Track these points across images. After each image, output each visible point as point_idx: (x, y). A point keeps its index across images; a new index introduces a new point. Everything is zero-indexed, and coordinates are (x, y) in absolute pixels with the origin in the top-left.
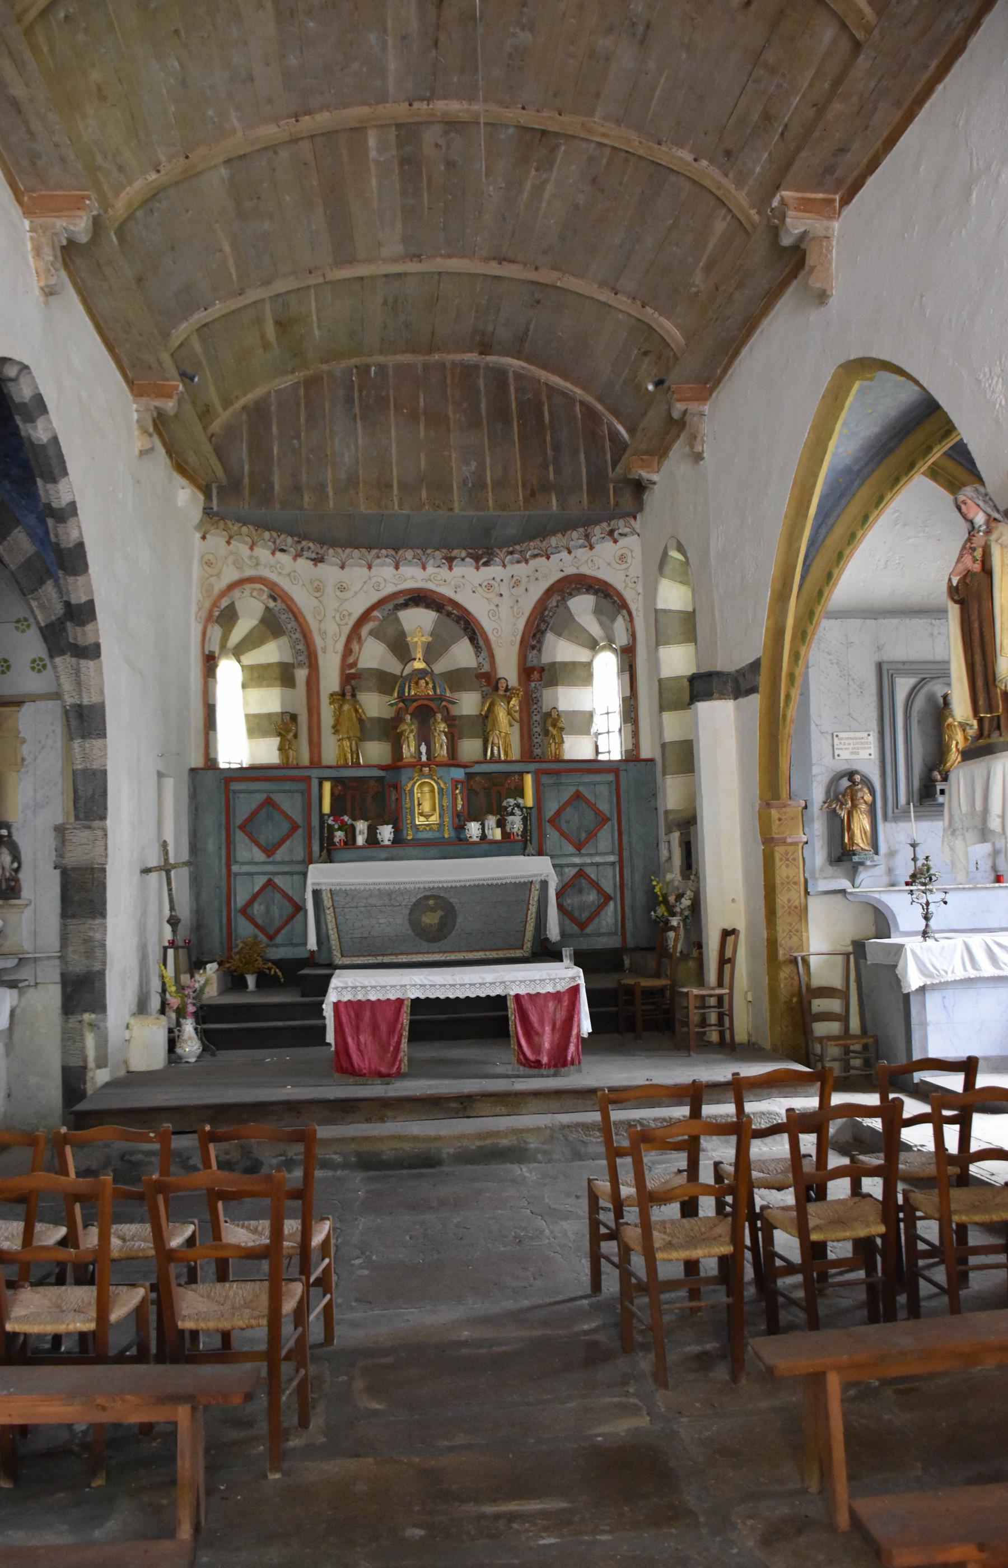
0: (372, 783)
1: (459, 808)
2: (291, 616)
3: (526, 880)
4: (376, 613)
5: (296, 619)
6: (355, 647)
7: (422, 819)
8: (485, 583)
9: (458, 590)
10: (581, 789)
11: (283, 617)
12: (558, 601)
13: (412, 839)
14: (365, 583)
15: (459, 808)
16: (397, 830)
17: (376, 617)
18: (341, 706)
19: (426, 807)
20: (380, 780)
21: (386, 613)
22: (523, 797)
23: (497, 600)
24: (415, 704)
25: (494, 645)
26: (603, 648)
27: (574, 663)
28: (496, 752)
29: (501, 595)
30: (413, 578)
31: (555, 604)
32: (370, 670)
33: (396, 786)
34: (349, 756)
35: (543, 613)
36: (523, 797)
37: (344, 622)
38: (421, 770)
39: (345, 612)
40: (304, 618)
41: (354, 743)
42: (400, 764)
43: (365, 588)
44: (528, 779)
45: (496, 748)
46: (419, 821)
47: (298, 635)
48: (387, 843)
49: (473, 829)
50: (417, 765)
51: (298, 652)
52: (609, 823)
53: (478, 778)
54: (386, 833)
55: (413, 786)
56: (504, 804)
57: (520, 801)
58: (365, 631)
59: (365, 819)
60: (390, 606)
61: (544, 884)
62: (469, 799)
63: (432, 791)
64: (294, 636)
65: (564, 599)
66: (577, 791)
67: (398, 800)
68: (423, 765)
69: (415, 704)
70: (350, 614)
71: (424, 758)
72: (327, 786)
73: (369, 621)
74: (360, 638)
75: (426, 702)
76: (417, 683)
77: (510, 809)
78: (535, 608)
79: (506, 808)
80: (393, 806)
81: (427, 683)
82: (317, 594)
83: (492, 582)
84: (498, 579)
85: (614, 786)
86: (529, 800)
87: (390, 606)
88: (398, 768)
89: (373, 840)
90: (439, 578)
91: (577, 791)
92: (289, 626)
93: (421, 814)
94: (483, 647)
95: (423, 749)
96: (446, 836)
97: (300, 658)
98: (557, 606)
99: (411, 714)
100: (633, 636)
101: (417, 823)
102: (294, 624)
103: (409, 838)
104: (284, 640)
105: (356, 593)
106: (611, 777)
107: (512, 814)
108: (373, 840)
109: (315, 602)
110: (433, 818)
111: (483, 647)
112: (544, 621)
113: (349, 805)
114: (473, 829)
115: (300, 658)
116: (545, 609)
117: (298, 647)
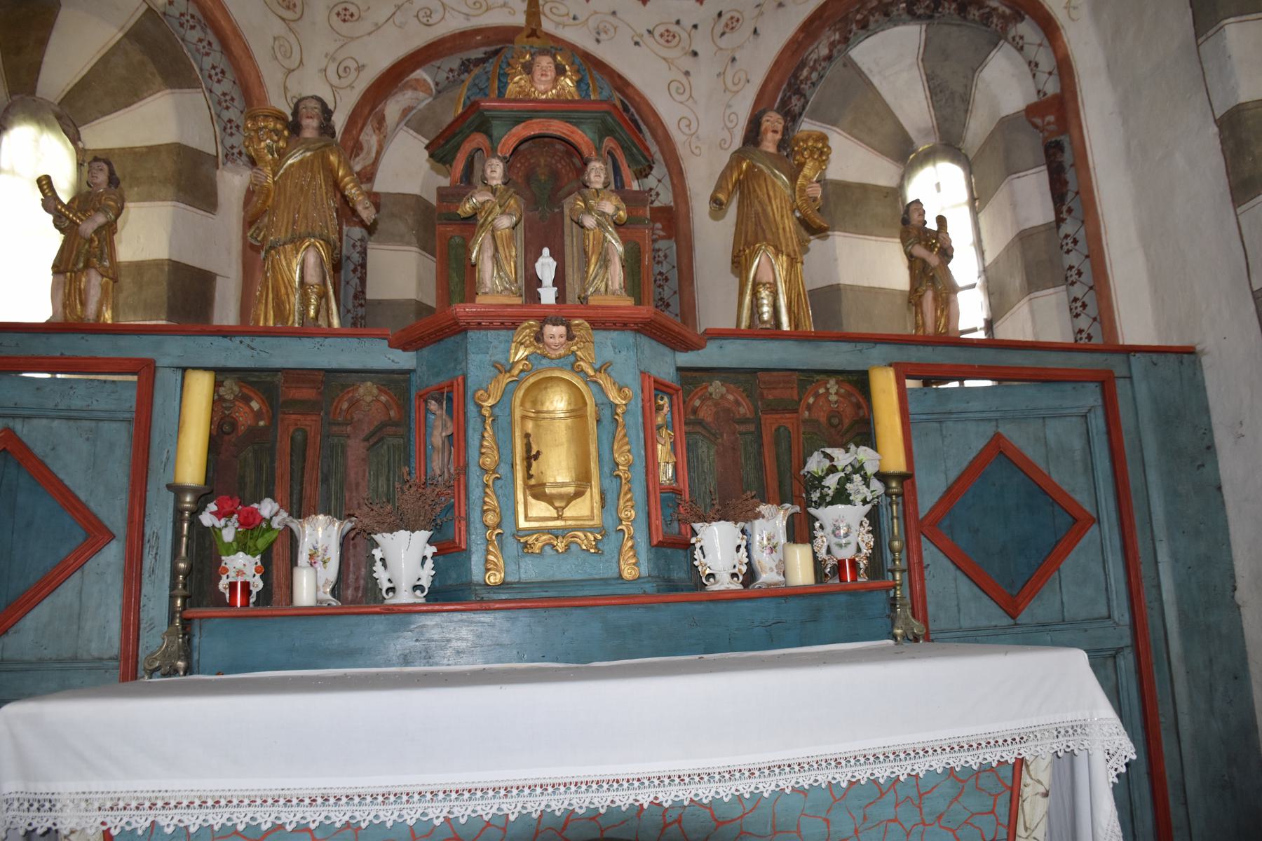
0: (366, 391)
1: (666, 474)
2: (211, 37)
3: (993, 756)
4: (420, 74)
5: (226, 48)
6: (370, 139)
7: (540, 509)
8: (661, 29)
9: (603, 36)
10: (1007, 430)
11: (193, 36)
12: (832, 45)
13: (504, 585)
14: (399, 7)
15: (666, 474)
16: (448, 550)
17: (418, 85)
18: (283, 154)
19: (558, 468)
20: (394, 381)
21: (442, 76)
22: (873, 445)
23: (687, 63)
24: (521, 131)
25: (682, 151)
26: (929, 157)
27: (864, 188)
28: (766, 310)
29: (695, 54)
30: (505, 5)
31: (824, 51)
32: (401, 199)
33: (451, 395)
34: (295, 299)
35: (795, 76)
36: (873, 445)
37: (345, 82)
38: (539, 337)
39: (353, 65)
40: (247, 49)
41: (312, 259)
42: (462, 310)
43: (398, 18)
44: (884, 386)
45: (764, 293)
46: (533, 514)
47: (226, 86)
48: (405, 597)
49: (718, 547)
50: (525, 313)
51: (228, 127)
52: (1093, 531)
53: (716, 387)
54: (405, 557)
55: (508, 393)
56: (815, 464)
57: (864, 454)
58: (392, 109)
59: (339, 513)
60: (454, 62)
61: (1066, 763)
62: (691, 448)
63: (577, 412)
64: (219, 89)
65: (846, 41)
66: (997, 437)
67: (457, 441)
68: (544, 320)
69: (521, 131)
70: (360, 68)
71: (548, 295)
72: (200, 388)
73: (406, 87)
74: (381, 120)
75: (557, 127)
76: (528, 69)
77: (832, 482)
78: (777, 64)
79: (816, 481)
80: (436, 464)
81: (560, 71)
82: (288, 15)
83: (674, 28)
84: (687, 23)
85: (1098, 422)
86: (891, 453)
87: (454, 62)
88: (457, 329)
89: (357, 588)
90: (563, 10)
91: (997, 437)
92: (207, 62)
93: (537, 491)
94: (658, 156)
95: (546, 267)
96: (628, 573)
97: (230, 141)
98: (829, 58)
99: (505, 160)
100: (1064, 68)
101: (522, 524)
102: (216, 58)
103: (494, 579)
104: (196, 99)
105: (378, 27)
106: (1091, 397)
107: (842, 496)
108: (357, 588)
109: (278, 28)
110: (582, 509)
111: (658, 156)
112: (799, 93)
113: (282, 466)
114: (718, 547)
115: (230, 141)
116: (803, 64)
117: (226, 115)
